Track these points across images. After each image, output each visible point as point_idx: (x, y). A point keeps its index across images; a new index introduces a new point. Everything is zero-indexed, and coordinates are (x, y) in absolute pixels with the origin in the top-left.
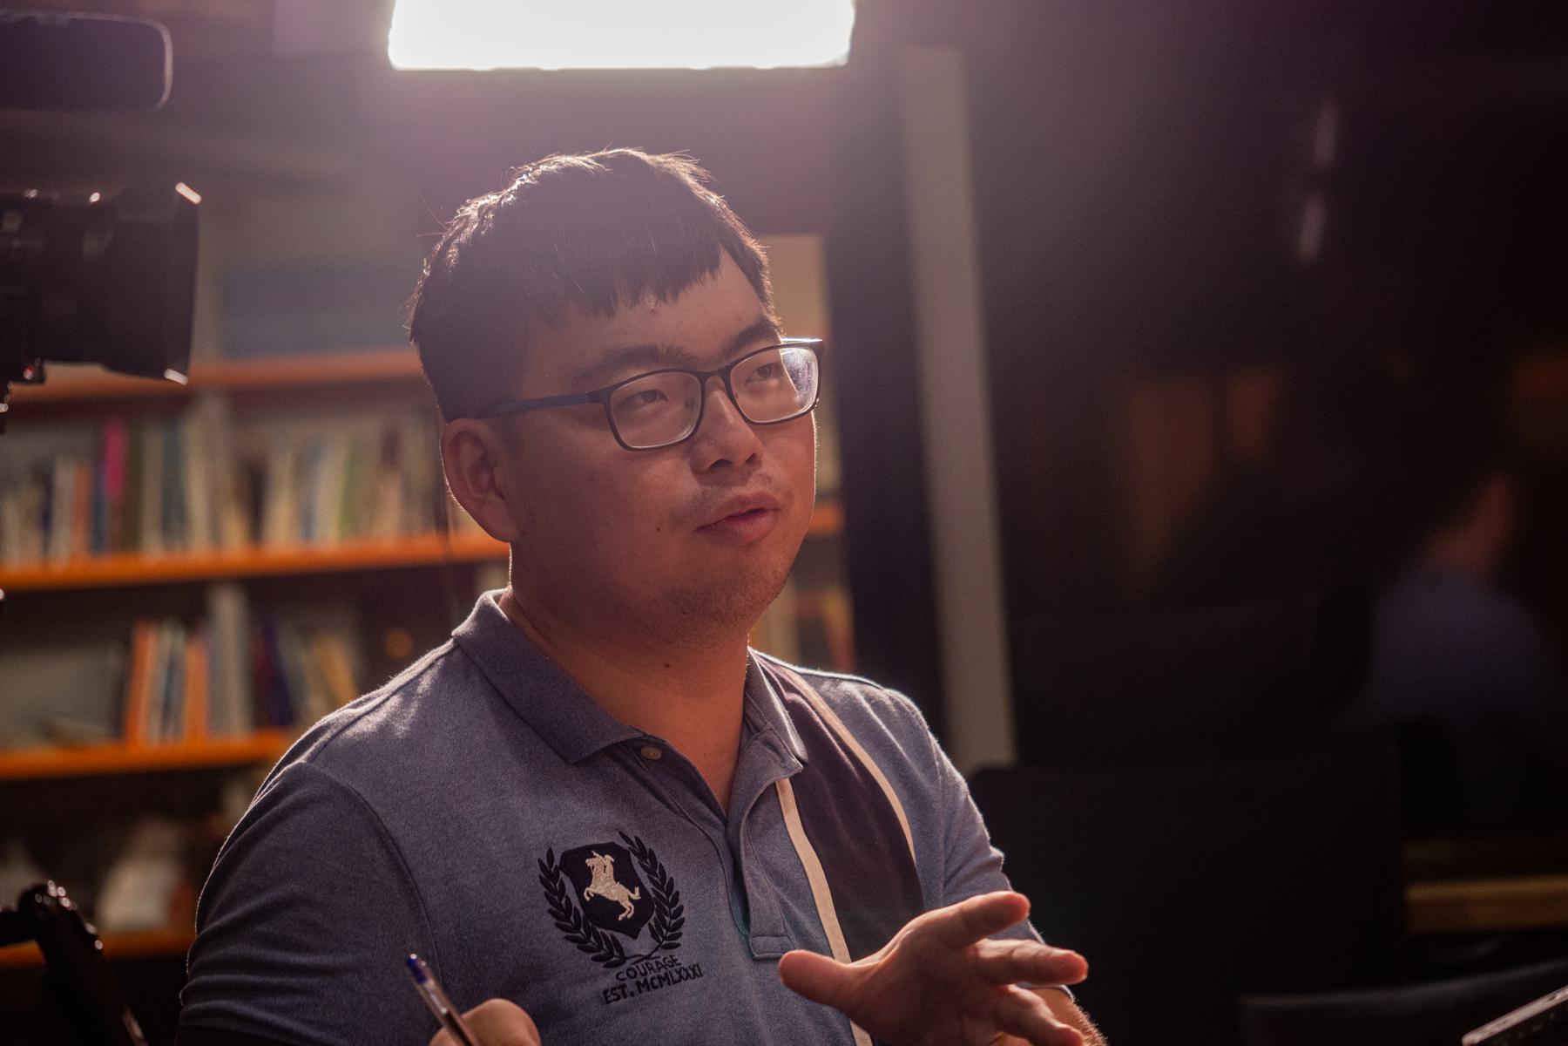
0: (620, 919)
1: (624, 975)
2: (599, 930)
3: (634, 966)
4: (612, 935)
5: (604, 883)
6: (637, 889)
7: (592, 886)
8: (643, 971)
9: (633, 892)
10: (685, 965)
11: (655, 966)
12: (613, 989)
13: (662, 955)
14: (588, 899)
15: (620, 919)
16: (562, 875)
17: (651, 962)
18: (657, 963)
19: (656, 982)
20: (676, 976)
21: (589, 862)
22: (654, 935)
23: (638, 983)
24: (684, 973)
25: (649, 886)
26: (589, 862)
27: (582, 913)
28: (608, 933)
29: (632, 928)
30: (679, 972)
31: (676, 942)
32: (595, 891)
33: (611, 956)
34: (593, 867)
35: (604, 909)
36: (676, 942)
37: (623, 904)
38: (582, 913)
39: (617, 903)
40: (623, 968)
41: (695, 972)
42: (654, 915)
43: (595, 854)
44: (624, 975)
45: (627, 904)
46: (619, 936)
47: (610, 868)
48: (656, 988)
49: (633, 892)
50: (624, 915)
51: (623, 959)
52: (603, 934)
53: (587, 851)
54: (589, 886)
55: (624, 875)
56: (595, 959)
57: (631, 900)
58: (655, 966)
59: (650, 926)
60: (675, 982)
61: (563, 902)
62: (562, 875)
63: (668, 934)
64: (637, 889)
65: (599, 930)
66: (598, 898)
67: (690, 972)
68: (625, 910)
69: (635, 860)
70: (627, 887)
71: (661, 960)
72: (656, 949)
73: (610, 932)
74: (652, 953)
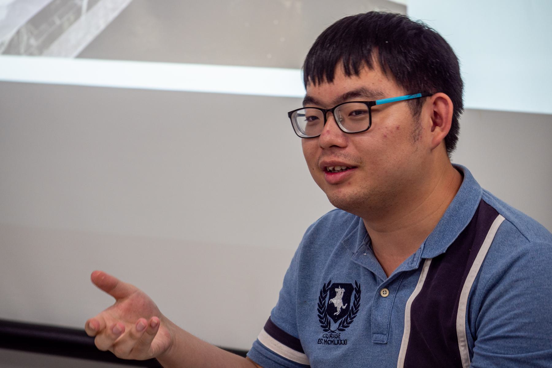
6: (346, 305)
8: (328, 336)
9: (344, 305)
14: (330, 303)
19: (329, 342)
21: (336, 290)
26: (336, 290)
27: (326, 308)
28: (329, 318)
34: (337, 292)
38: (326, 308)
46: (332, 321)
49: (344, 305)
55: (346, 299)
57: (341, 308)
66: (333, 304)
69: (354, 292)
73: (330, 318)
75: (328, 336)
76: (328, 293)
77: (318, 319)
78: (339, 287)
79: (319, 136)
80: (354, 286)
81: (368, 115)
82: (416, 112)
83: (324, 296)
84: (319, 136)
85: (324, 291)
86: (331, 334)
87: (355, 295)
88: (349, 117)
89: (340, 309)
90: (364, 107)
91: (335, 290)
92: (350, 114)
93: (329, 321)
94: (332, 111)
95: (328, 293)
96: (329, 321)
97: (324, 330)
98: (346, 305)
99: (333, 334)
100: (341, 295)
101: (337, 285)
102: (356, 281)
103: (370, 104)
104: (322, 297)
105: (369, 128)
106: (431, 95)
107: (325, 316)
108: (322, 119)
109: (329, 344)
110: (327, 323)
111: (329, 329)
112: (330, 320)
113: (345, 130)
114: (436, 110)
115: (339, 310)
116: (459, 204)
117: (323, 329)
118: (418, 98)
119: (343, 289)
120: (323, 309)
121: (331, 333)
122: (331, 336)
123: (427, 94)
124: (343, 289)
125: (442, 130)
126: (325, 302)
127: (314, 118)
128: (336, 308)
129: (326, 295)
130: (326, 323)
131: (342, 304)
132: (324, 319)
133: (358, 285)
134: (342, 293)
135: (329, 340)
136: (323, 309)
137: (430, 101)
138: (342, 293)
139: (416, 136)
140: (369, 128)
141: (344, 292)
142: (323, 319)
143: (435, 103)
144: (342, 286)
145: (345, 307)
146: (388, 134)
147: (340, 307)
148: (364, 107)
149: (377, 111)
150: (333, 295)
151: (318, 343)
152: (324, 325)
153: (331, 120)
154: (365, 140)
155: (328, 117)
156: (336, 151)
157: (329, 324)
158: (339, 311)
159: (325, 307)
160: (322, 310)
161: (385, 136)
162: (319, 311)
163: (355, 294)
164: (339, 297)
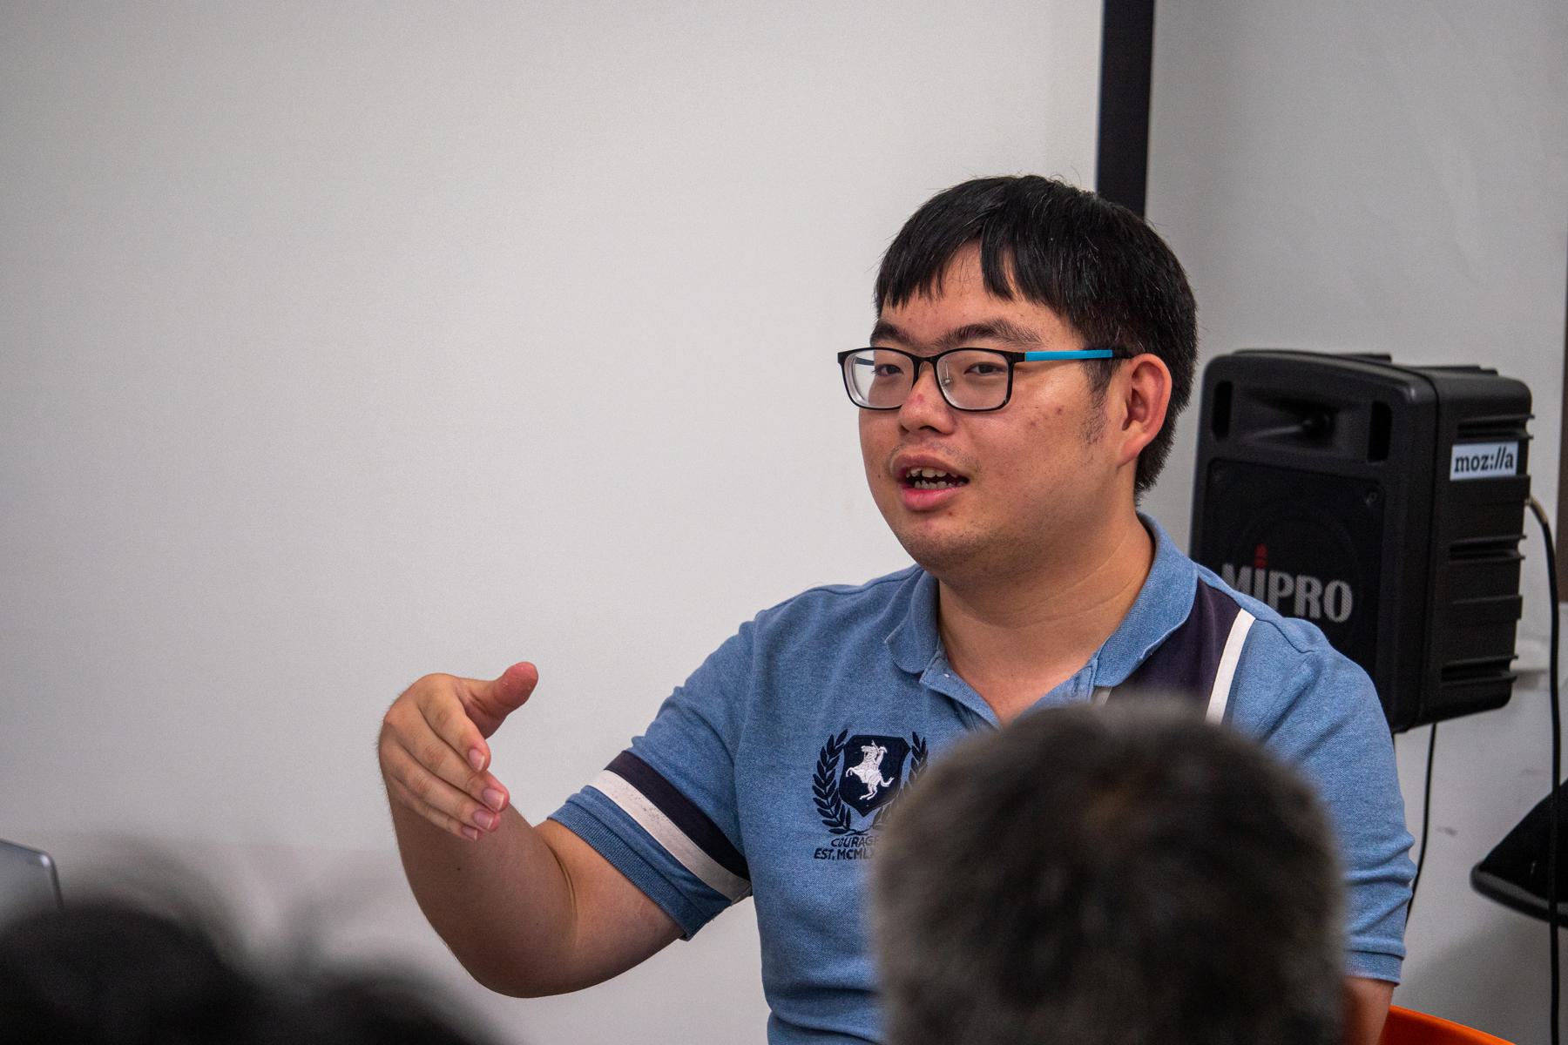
2: (842, 802)
6: (891, 779)
8: (847, 843)
9: (886, 781)
14: (847, 776)
19: (852, 854)
21: (865, 749)
26: (865, 749)
27: (837, 786)
28: (847, 806)
33: (839, 824)
34: (867, 754)
38: (837, 786)
46: (854, 811)
49: (886, 781)
50: (864, 796)
52: (843, 806)
53: (867, 740)
55: (890, 768)
57: (879, 786)
65: (842, 802)
66: (856, 778)
69: (910, 755)
73: (849, 806)
75: (847, 843)
76: (842, 755)
77: (816, 807)
78: (873, 744)
79: (899, 407)
80: (911, 743)
81: (1005, 376)
82: (1099, 386)
83: (831, 761)
84: (899, 407)
85: (831, 750)
86: (854, 838)
87: (913, 761)
88: (965, 376)
89: (875, 789)
90: (1000, 360)
91: (861, 749)
92: (969, 370)
93: (846, 811)
94: (934, 361)
95: (842, 755)
96: (846, 811)
97: (831, 831)
98: (891, 779)
99: (860, 837)
100: (876, 759)
101: (867, 740)
102: (914, 733)
103: (1014, 359)
104: (825, 764)
105: (1004, 404)
106: (1129, 356)
107: (836, 802)
108: (908, 373)
109: (851, 858)
110: (841, 816)
111: (848, 828)
112: (849, 811)
113: (954, 403)
114: (1136, 387)
115: (873, 788)
116: (1163, 582)
117: (830, 828)
118: (1105, 360)
119: (881, 748)
120: (828, 788)
121: (855, 836)
122: (853, 842)
123: (1124, 354)
124: (883, 748)
125: (1145, 430)
126: (833, 775)
127: (893, 369)
128: (866, 785)
129: (835, 763)
130: (838, 816)
131: (880, 778)
132: (833, 808)
133: (921, 740)
134: (878, 755)
135: (851, 851)
136: (828, 788)
137: (1127, 367)
138: (878, 755)
139: (1092, 433)
140: (1004, 404)
141: (885, 754)
142: (829, 807)
143: (1136, 375)
144: (880, 741)
145: (889, 783)
146: (1038, 420)
147: (876, 784)
148: (1000, 360)
149: (1026, 371)
150: (856, 758)
151: (816, 857)
152: (834, 820)
153: (926, 380)
154: (994, 427)
155: (922, 371)
156: (933, 440)
157: (847, 818)
158: (874, 792)
159: (835, 783)
160: (825, 790)
161: (1033, 424)
162: (817, 792)
163: (913, 759)
164: (871, 764)
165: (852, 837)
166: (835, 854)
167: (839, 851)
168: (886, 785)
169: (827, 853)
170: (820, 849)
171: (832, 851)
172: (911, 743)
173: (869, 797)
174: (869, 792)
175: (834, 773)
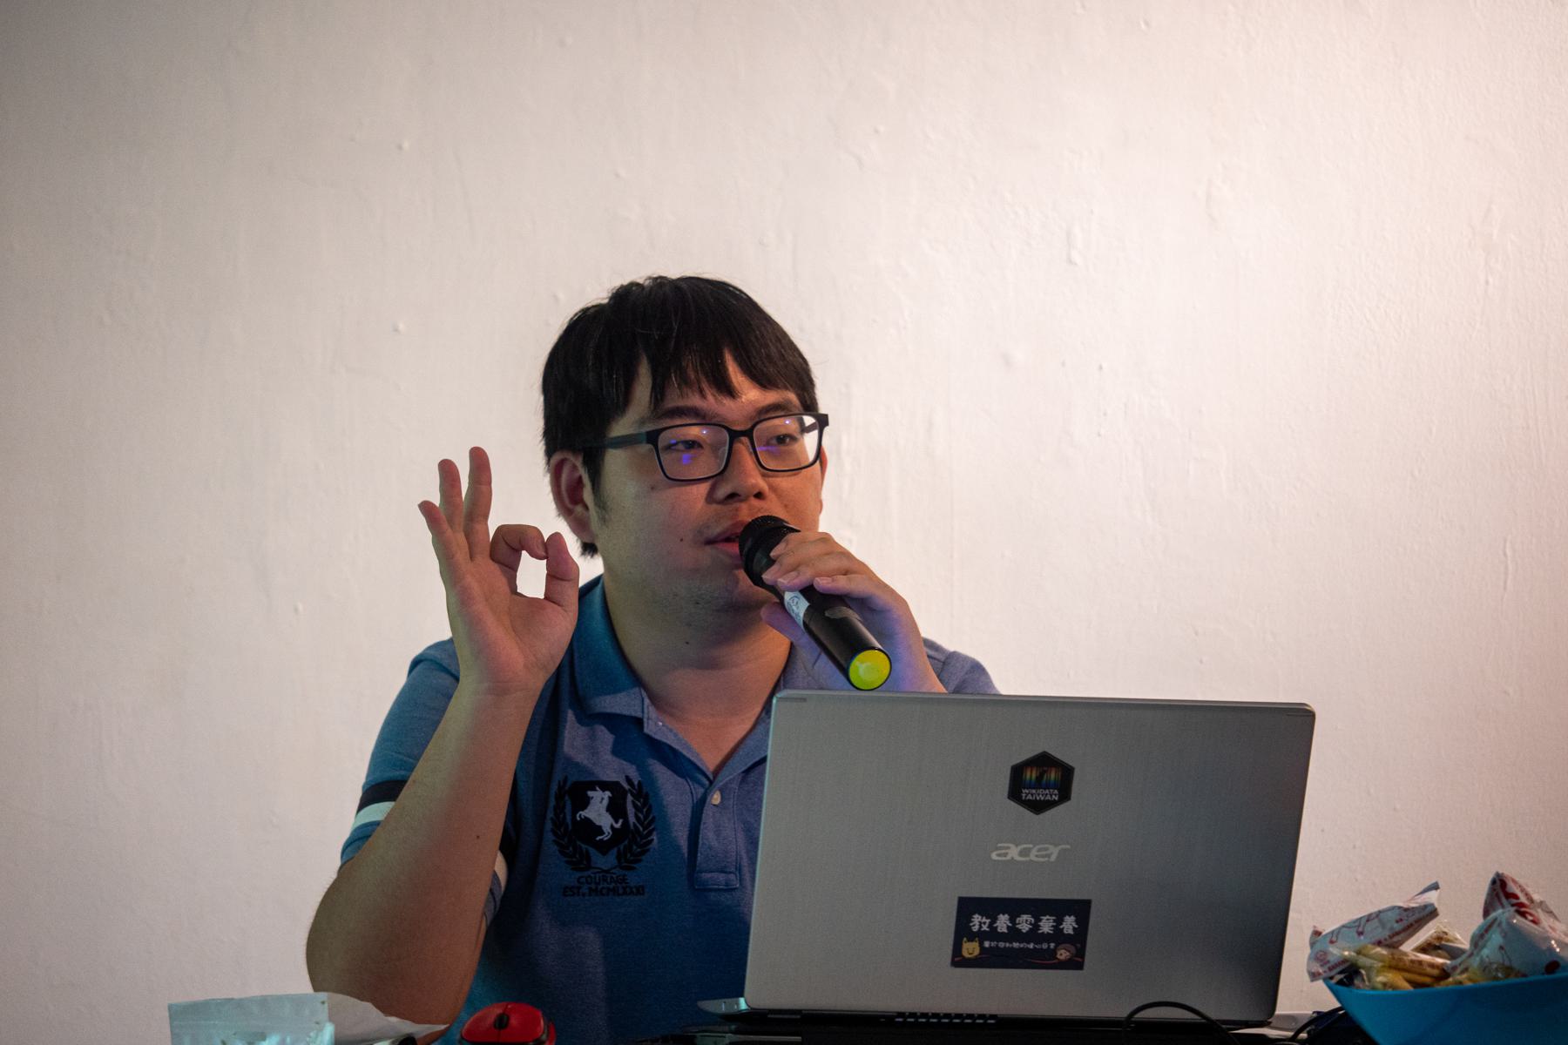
0: (598, 838)
1: (583, 880)
3: (592, 875)
4: (587, 851)
5: (598, 811)
6: (621, 821)
7: (586, 811)
8: (597, 881)
9: (617, 822)
10: (632, 884)
11: (609, 881)
12: (573, 887)
13: (618, 872)
14: (578, 819)
15: (598, 838)
16: (567, 798)
17: (608, 875)
18: (612, 878)
19: (604, 891)
20: (621, 891)
21: (590, 793)
22: (619, 857)
23: (590, 889)
24: (628, 890)
25: (632, 819)
26: (590, 793)
27: (570, 828)
29: (604, 848)
30: (624, 888)
31: (635, 866)
32: (587, 815)
33: (580, 862)
34: (592, 798)
35: (592, 828)
36: (635, 866)
37: (604, 830)
38: (570, 828)
39: (600, 827)
40: (585, 874)
41: (640, 890)
42: (626, 842)
43: (597, 788)
44: (583, 880)
45: (607, 829)
46: (592, 851)
47: (606, 802)
48: (603, 895)
49: (617, 822)
50: (601, 837)
51: (589, 867)
52: (581, 847)
54: (583, 810)
55: (615, 809)
56: (567, 862)
57: (612, 827)
58: (609, 881)
59: (619, 851)
60: (619, 895)
61: (561, 816)
62: (567, 798)
63: (629, 860)
64: (621, 821)
65: (579, 843)
66: (587, 821)
67: (634, 890)
68: (604, 833)
69: (630, 798)
70: (613, 817)
71: (614, 876)
72: (615, 868)
73: (586, 846)
74: (612, 869)
80: (627, 787)
86: (603, 876)
100: (601, 802)
141: (609, 797)
144: (604, 786)
150: (585, 803)
152: (574, 860)
165: (601, 875)
166: (585, 889)
167: (590, 889)
168: (618, 826)
169: (576, 891)
170: (567, 887)
171: (579, 888)
172: (627, 787)
173: (605, 837)
174: (604, 833)
175: (565, 814)
